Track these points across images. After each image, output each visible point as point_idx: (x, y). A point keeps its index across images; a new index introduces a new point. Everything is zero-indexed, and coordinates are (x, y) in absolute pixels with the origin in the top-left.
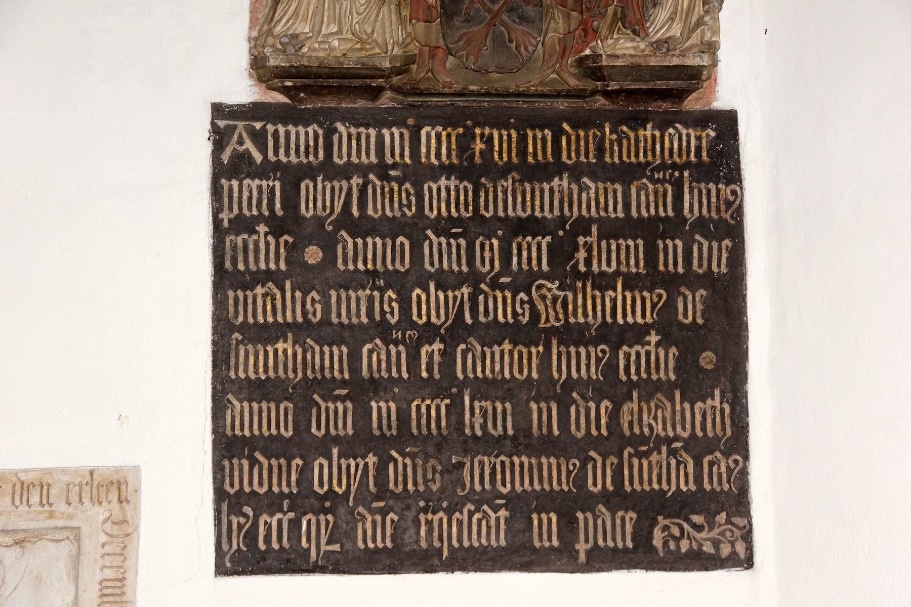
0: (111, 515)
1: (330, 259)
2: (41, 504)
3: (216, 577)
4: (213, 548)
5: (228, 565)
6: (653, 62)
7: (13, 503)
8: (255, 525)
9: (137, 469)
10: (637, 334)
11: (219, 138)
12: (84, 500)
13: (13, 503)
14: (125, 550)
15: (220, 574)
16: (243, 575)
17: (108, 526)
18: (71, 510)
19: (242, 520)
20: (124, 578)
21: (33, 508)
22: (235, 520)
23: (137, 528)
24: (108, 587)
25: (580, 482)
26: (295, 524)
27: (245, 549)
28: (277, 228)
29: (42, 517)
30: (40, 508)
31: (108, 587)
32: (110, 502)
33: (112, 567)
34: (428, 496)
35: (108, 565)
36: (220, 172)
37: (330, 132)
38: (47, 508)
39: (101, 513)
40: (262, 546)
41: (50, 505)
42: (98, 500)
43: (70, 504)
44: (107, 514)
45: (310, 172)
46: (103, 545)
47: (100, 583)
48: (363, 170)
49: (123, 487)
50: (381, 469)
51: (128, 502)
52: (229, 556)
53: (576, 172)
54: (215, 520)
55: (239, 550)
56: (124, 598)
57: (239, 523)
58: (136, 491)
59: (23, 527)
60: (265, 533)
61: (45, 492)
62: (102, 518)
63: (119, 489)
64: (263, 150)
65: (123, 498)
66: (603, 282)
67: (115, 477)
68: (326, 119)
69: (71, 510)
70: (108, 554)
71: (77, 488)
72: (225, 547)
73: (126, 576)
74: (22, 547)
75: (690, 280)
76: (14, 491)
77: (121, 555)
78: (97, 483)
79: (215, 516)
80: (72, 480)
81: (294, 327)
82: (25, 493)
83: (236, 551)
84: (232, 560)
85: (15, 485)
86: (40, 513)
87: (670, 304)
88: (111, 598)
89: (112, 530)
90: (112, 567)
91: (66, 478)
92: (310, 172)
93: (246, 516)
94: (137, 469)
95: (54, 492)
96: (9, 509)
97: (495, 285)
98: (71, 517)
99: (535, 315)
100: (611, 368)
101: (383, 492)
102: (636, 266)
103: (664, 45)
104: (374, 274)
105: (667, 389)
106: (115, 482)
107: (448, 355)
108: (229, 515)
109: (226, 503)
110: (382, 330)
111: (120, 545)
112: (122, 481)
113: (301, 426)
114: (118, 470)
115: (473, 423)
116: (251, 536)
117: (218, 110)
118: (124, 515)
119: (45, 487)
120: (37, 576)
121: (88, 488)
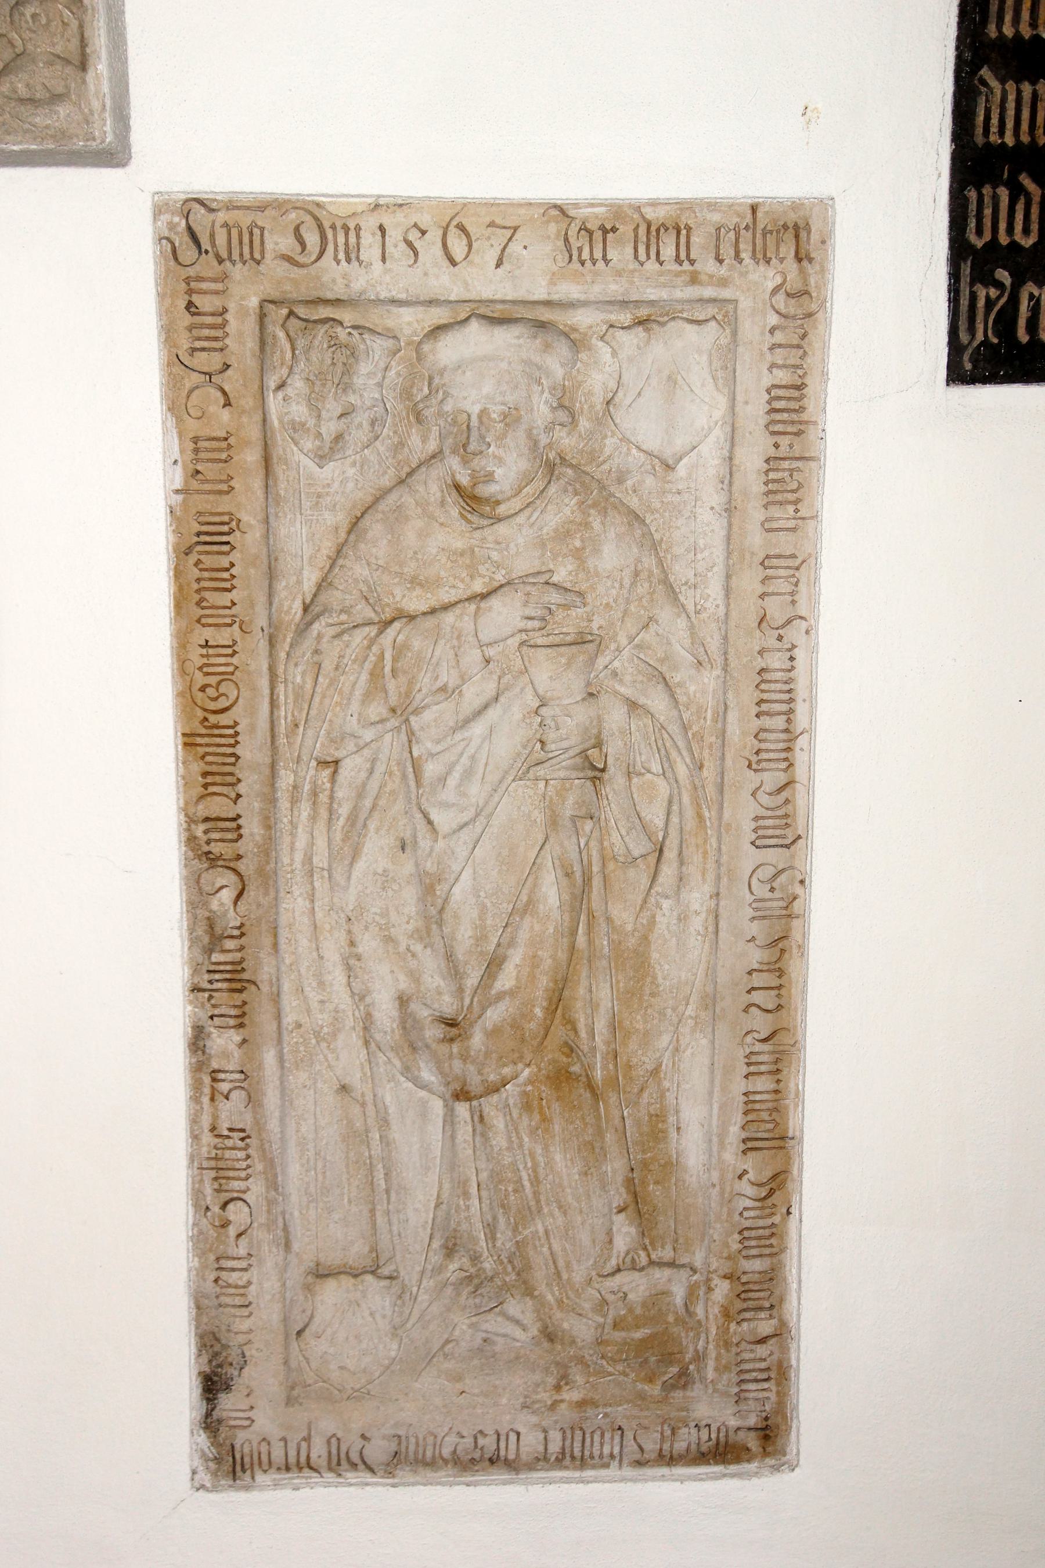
0: (785, 281)
2: (678, 260)
3: (948, 385)
4: (945, 339)
5: (968, 366)
7: (636, 257)
8: (1014, 301)
9: (825, 204)
12: (743, 255)
13: (636, 257)
14: (806, 340)
15: (954, 382)
16: (990, 383)
17: (780, 300)
18: (723, 271)
19: (993, 292)
20: (803, 383)
21: (667, 266)
22: (982, 293)
23: (823, 304)
24: (779, 398)
27: (995, 341)
29: (679, 281)
30: (676, 267)
31: (779, 398)
32: (782, 260)
33: (784, 366)
35: (780, 362)
38: (686, 266)
39: (767, 278)
40: (1023, 337)
41: (692, 262)
42: (765, 255)
43: (721, 262)
44: (779, 280)
46: (772, 331)
47: (768, 391)
49: (803, 235)
51: (810, 260)
52: (970, 351)
54: (949, 292)
55: (986, 343)
56: (804, 417)
57: (988, 297)
58: (823, 242)
59: (652, 297)
60: (1030, 314)
61: (683, 240)
62: (770, 285)
63: (797, 237)
65: (802, 255)
67: (792, 218)
69: (723, 271)
70: (780, 346)
71: (732, 235)
72: (964, 337)
73: (806, 381)
74: (647, 330)
76: (636, 236)
77: (799, 347)
78: (762, 226)
79: (950, 285)
80: (723, 221)
82: (653, 240)
83: (982, 344)
84: (974, 361)
85: (638, 225)
86: (678, 274)
88: (785, 416)
89: (786, 306)
90: (784, 366)
91: (716, 217)
93: (999, 285)
94: (825, 204)
95: (697, 240)
96: (631, 267)
98: (723, 283)
106: (791, 225)
108: (972, 284)
109: (969, 263)
111: (797, 330)
112: (801, 224)
114: (796, 206)
116: (1006, 321)
118: (806, 283)
119: (684, 232)
120: (669, 377)
121: (749, 235)
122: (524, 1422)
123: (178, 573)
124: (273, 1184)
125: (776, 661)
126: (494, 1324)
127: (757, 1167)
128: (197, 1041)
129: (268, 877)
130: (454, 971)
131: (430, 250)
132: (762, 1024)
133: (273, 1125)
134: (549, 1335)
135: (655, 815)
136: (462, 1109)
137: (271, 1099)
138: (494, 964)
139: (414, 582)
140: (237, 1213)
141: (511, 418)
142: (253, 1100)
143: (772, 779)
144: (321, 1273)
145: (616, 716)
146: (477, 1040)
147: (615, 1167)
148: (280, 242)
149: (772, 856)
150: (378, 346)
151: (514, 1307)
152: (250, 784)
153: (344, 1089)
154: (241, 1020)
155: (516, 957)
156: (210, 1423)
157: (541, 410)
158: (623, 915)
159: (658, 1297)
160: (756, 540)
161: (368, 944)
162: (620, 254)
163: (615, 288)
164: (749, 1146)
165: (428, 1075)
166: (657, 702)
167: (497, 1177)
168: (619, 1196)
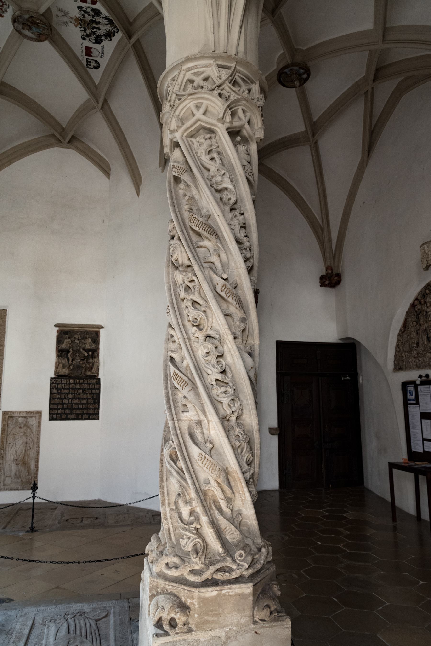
6: (92, 375)
9: (42, 411)
10: (90, 399)
11: (51, 380)
25: (84, 412)
26: (56, 416)
28: (56, 389)
36: (51, 384)
37: (62, 380)
45: (59, 384)
48: (65, 383)
50: (65, 411)
53: (85, 384)
66: (87, 394)
68: (61, 379)
75: (95, 394)
92: (59, 384)
94: (42, 411)
97: (77, 394)
99: (80, 397)
100: (87, 402)
102: (90, 392)
103: (93, 373)
104: (65, 393)
105: (92, 404)
107: (72, 401)
110: (65, 398)
113: (57, 407)
115: (74, 407)
116: (52, 417)
117: (51, 378)
125: (38, 437)
126: (18, 480)
127: (36, 469)
129: (5, 451)
130: (17, 456)
131: (18, 414)
132: (37, 459)
133: (4, 466)
134: (22, 481)
135: (31, 446)
136: (17, 466)
137: (4, 465)
138: (19, 456)
139: (16, 432)
141: (23, 422)
142: (3, 465)
143: (38, 444)
144: (6, 477)
145: (28, 440)
146: (18, 461)
147: (27, 469)
148: (9, 413)
149: (38, 449)
150: (15, 419)
151: (20, 479)
152: (5, 444)
153: (9, 464)
154: (3, 459)
155: (21, 455)
158: (28, 453)
159: (29, 478)
160: (37, 429)
161: (11, 455)
162: (30, 414)
164: (36, 467)
165: (15, 463)
166: (31, 439)
167: (19, 470)
168: (27, 471)
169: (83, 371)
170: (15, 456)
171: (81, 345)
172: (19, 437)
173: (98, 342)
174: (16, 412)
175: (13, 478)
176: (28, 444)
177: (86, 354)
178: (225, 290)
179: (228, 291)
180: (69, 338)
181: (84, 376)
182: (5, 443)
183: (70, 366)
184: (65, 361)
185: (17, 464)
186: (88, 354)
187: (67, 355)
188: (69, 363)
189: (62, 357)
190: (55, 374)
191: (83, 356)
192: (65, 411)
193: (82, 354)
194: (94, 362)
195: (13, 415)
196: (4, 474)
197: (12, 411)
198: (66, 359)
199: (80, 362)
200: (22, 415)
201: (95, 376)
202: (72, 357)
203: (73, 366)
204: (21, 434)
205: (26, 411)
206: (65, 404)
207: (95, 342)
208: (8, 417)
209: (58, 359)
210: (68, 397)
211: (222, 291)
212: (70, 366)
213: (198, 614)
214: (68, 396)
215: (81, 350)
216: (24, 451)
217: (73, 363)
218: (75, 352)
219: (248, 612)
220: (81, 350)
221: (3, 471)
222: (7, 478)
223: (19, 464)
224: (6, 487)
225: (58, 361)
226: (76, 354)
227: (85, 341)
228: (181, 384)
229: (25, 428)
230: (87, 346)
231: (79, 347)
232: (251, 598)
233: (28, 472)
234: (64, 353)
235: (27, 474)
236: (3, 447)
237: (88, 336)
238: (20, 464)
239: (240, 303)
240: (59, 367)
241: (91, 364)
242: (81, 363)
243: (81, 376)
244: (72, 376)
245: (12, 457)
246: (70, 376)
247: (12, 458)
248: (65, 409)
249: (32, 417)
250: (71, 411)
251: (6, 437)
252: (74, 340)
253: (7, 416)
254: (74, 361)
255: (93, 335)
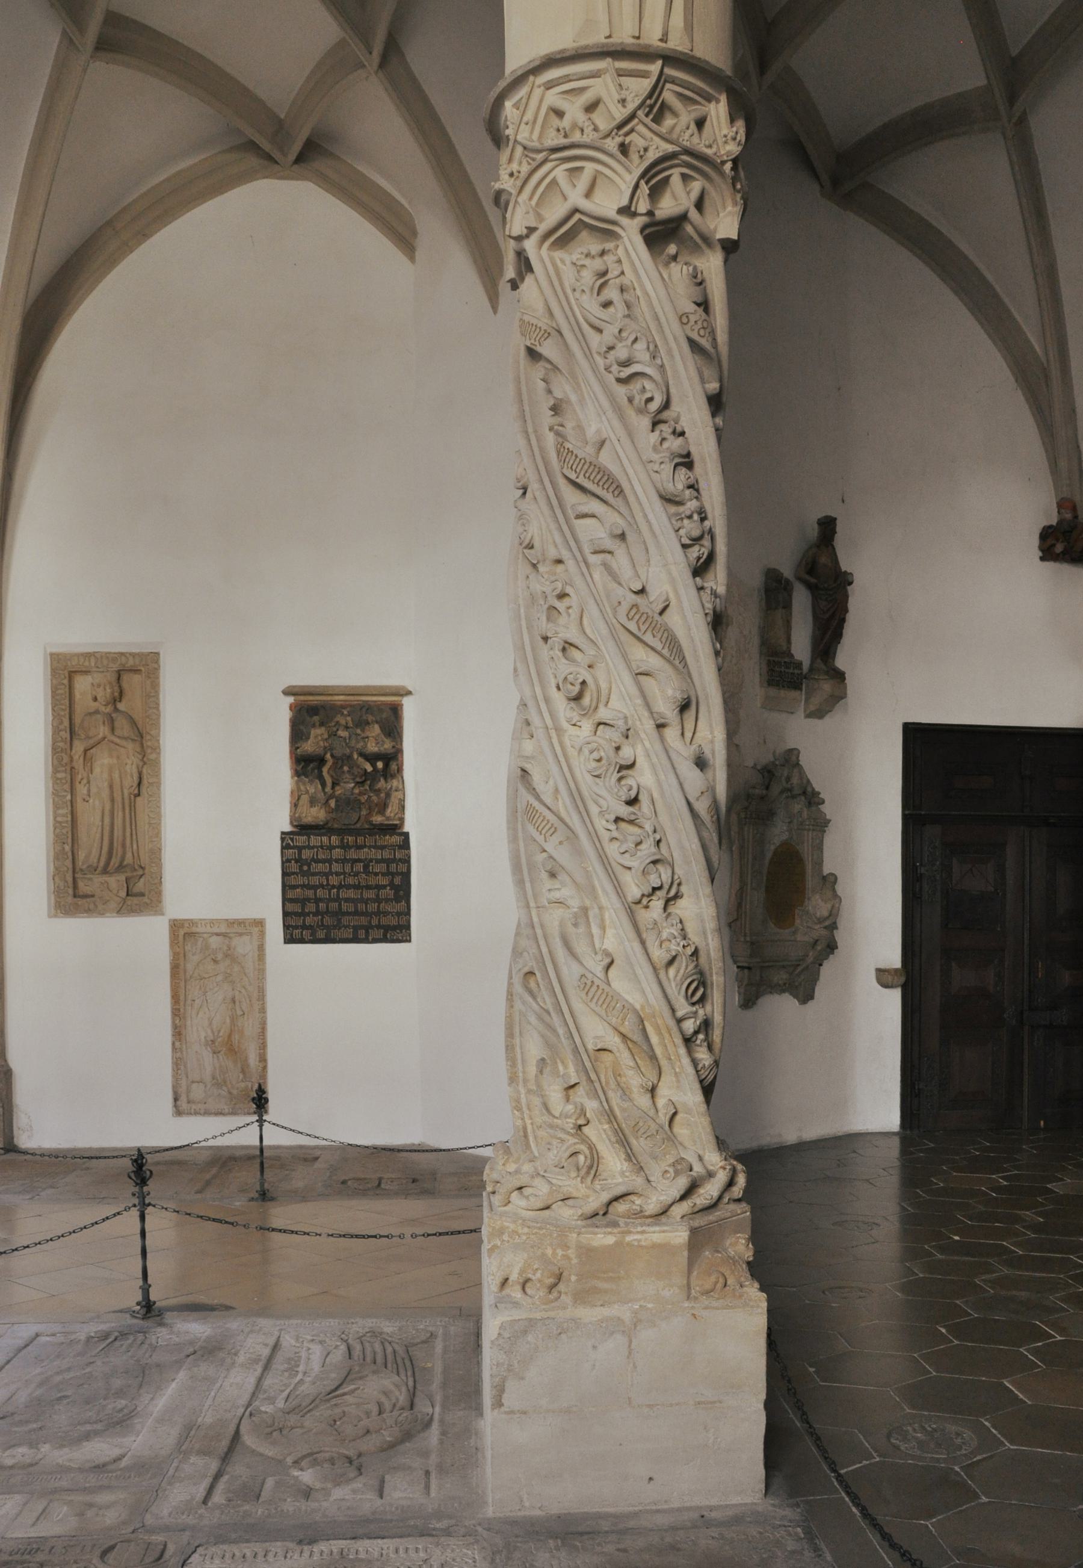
1: (309, 868)
6: (386, 822)
10: (384, 887)
11: (283, 840)
25: (370, 922)
26: (302, 933)
28: (297, 861)
34: (334, 926)
36: (283, 848)
37: (309, 838)
39: (256, 929)
45: (304, 847)
48: (317, 847)
50: (322, 920)
53: (370, 847)
64: (293, 842)
75: (398, 874)
81: (301, 885)
87: (393, 880)
97: (350, 875)
100: (378, 895)
101: (323, 925)
102: (384, 870)
103: (388, 819)
105: (391, 900)
107: (338, 892)
110: (322, 886)
113: (303, 909)
116: (292, 935)
117: (283, 833)
122: (225, 1107)
123: (171, 972)
124: (185, 1067)
126: (220, 1091)
127: (261, 1065)
128: (173, 1044)
129: (185, 1018)
130: (213, 1032)
131: (208, 926)
134: (230, 1093)
138: (219, 1031)
140: (179, 1072)
141: (220, 949)
142: (182, 1053)
144: (193, 1082)
147: (239, 1065)
148: (187, 925)
151: (224, 1088)
152: (182, 1003)
156: (175, 1106)
157: (225, 948)
158: (240, 1024)
162: (235, 926)
163: (234, 931)
164: (260, 1061)
166: (243, 991)
169: (364, 812)
170: (209, 1031)
171: (353, 743)
172: (215, 984)
173: (398, 733)
174: (203, 923)
175: (209, 1086)
176: (237, 1003)
177: (369, 769)
178: (637, 617)
179: (643, 619)
180: (322, 724)
181: (367, 826)
182: (182, 997)
183: (327, 801)
184: (316, 788)
185: (214, 1053)
186: (374, 765)
187: (321, 772)
188: (325, 793)
189: (307, 777)
190: (291, 823)
191: (362, 772)
192: (322, 920)
193: (358, 767)
194: (391, 788)
195: (194, 929)
196: (187, 1077)
197: (191, 920)
198: (317, 781)
199: (353, 788)
200: (216, 930)
201: (396, 825)
202: (332, 777)
203: (337, 801)
204: (220, 978)
205: (227, 920)
206: (321, 900)
207: (390, 735)
208: (185, 934)
209: (297, 783)
210: (328, 884)
211: (629, 619)
212: (327, 801)
213: (577, 1275)
214: (328, 880)
215: (355, 756)
216: (228, 1021)
217: (337, 793)
218: (340, 762)
219: (679, 1280)
220: (355, 756)
221: (182, 1067)
222: (194, 1086)
223: (219, 1052)
224: (194, 1107)
225: (299, 789)
226: (342, 767)
227: (363, 731)
228: (547, 832)
229: (228, 962)
230: (369, 745)
231: (349, 747)
232: (686, 1253)
233: (243, 1071)
234: (311, 765)
235: (241, 1076)
236: (179, 1010)
237: (370, 718)
238: (222, 1052)
239: (671, 647)
240: (301, 803)
241: (383, 795)
242: (357, 791)
243: (358, 826)
244: (336, 826)
245: (203, 1035)
246: (329, 828)
247: (203, 1040)
248: (322, 914)
249: (241, 935)
250: (339, 920)
251: (182, 984)
252: (335, 729)
253: (182, 932)
254: (337, 788)
255: (384, 715)
